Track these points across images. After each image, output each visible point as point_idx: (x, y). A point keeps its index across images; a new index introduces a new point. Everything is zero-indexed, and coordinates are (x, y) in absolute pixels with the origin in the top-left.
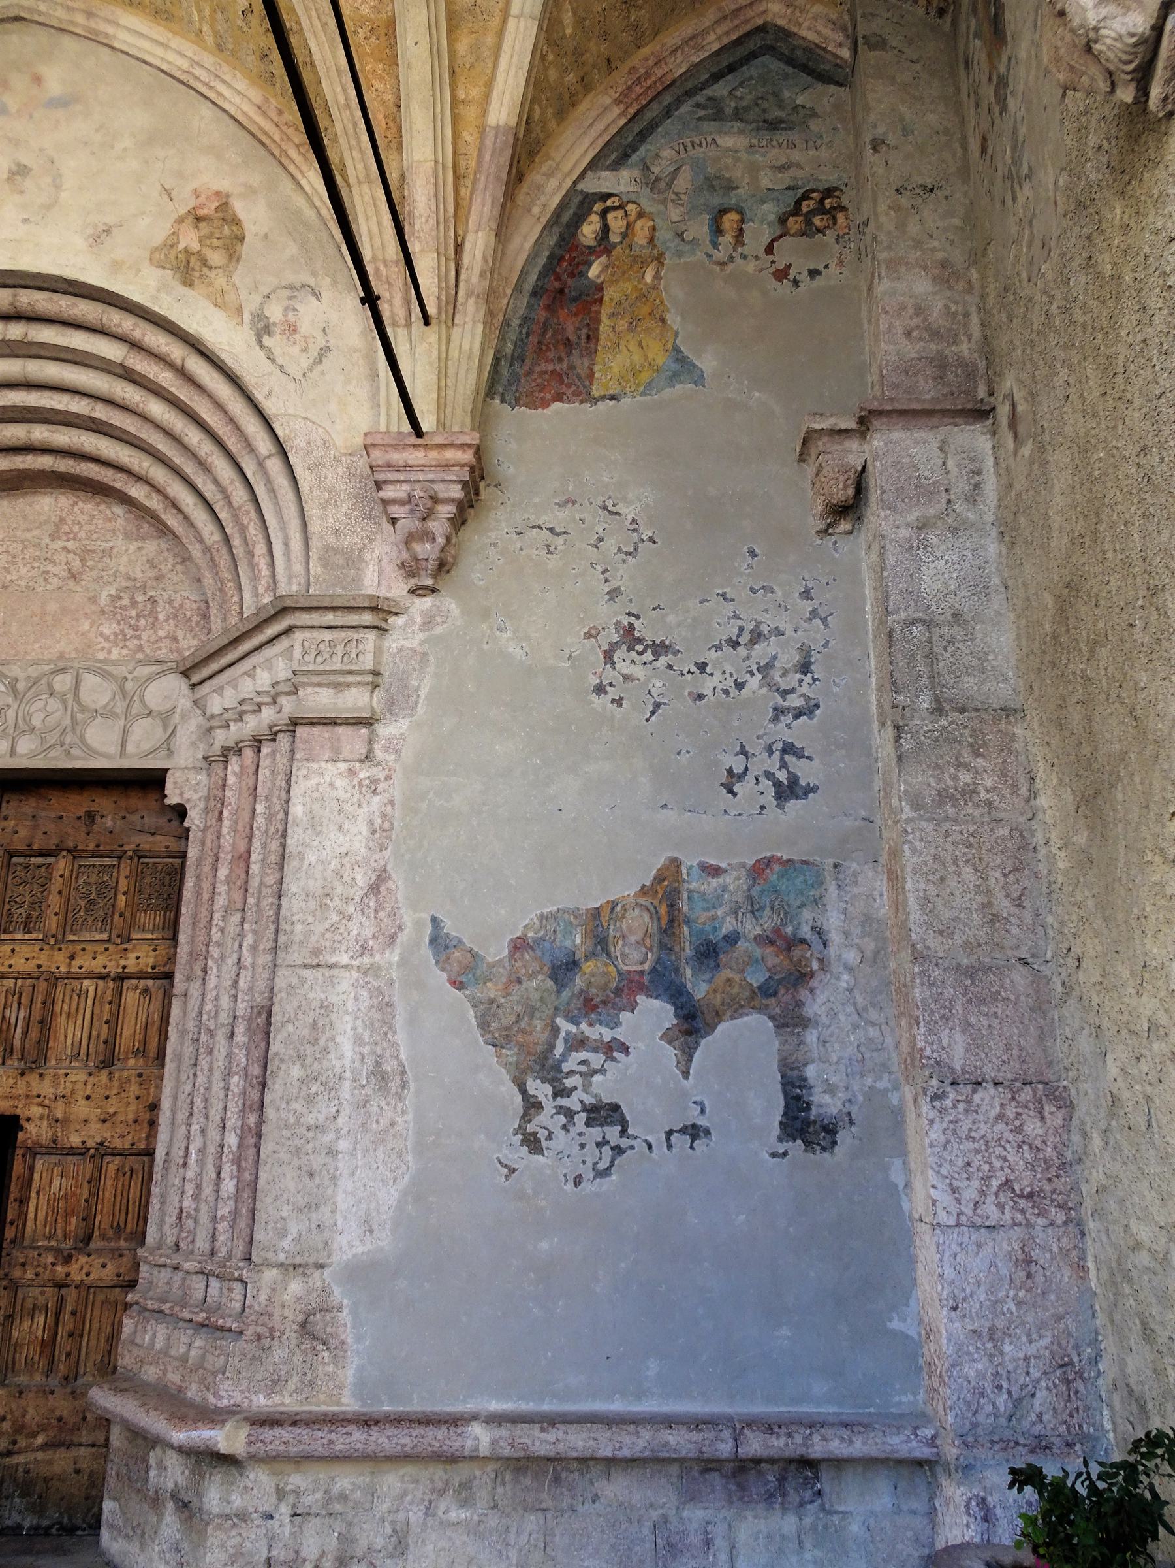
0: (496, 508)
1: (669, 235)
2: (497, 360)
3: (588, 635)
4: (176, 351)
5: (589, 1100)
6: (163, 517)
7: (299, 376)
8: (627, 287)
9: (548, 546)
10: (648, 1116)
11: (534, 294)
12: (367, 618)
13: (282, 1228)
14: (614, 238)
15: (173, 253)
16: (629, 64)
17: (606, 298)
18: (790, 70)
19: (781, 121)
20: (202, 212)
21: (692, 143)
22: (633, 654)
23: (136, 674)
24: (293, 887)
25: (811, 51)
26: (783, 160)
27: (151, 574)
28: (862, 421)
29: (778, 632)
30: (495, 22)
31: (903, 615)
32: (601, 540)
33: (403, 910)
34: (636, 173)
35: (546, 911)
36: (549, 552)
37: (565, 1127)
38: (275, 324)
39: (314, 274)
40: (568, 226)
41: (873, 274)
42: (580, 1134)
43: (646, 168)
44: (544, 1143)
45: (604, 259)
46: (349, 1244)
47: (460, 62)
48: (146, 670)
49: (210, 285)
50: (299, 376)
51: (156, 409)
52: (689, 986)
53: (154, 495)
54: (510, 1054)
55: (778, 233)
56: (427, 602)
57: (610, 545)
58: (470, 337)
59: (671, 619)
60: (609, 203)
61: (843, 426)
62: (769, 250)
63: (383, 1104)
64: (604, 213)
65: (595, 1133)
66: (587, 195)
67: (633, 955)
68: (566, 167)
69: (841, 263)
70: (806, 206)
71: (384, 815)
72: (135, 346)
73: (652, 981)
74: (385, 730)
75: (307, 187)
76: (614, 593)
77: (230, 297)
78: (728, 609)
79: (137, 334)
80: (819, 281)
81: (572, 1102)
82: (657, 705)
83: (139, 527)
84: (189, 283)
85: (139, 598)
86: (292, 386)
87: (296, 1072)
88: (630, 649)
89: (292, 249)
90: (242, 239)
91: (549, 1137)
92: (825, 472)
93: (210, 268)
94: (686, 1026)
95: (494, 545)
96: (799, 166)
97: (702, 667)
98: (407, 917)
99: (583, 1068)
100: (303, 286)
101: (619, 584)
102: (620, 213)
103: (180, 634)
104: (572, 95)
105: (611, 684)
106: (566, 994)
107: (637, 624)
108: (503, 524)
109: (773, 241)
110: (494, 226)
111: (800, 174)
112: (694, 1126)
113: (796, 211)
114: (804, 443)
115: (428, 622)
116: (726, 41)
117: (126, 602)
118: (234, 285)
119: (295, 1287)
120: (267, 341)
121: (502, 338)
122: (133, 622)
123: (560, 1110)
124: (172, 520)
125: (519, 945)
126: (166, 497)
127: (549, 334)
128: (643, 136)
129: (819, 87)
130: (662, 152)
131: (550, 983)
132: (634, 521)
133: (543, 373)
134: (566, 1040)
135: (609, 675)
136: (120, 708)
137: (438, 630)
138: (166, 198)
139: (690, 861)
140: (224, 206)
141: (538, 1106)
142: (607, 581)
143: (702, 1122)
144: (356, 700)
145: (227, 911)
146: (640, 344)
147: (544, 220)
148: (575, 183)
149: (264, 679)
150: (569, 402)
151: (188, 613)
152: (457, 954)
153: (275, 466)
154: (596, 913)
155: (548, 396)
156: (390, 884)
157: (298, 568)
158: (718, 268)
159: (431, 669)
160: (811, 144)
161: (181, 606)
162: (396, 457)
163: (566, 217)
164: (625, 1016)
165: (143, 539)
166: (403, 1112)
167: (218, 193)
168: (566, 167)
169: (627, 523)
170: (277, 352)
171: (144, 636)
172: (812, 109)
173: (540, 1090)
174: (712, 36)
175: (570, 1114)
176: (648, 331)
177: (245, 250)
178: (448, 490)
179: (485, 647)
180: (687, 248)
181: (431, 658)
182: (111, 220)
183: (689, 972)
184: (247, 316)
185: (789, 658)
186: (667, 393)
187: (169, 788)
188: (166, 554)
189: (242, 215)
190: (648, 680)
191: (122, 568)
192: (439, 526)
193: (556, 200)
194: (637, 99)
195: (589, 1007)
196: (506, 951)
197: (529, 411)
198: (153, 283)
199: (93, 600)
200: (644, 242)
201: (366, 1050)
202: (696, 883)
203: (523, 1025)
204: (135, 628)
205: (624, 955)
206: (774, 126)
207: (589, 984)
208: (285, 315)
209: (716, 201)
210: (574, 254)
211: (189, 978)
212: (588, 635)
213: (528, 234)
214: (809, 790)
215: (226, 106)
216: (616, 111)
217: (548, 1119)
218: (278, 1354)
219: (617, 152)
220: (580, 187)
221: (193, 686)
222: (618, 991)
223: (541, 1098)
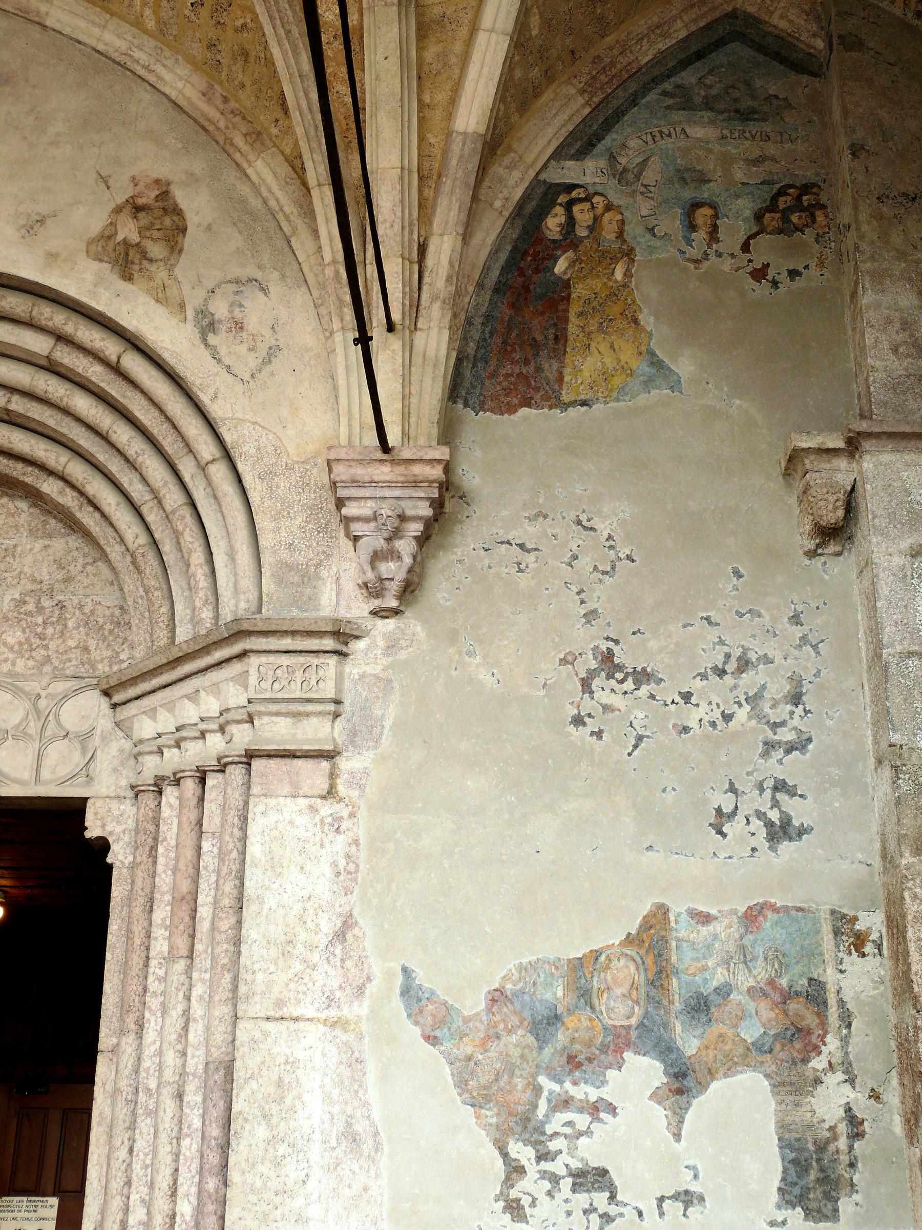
0: (461, 522)
1: (640, 230)
2: (459, 361)
3: (564, 661)
4: (111, 348)
5: (575, 1164)
6: (79, 515)
7: (247, 377)
8: (596, 284)
9: (519, 564)
10: (638, 1182)
11: (496, 290)
12: (329, 643)
14: (582, 232)
15: (111, 244)
16: (593, 53)
17: (573, 296)
18: (761, 58)
19: (753, 111)
20: (140, 201)
21: (661, 132)
22: (613, 682)
23: (50, 690)
24: (252, 931)
25: (782, 39)
26: (757, 153)
27: (60, 576)
28: (850, 441)
29: (767, 660)
30: (464, 32)
31: (899, 648)
32: (575, 557)
33: (372, 959)
34: (603, 163)
35: (525, 961)
36: (520, 571)
37: (550, 1194)
38: (220, 321)
39: (261, 267)
40: (531, 216)
41: (856, 283)
42: (566, 1201)
43: (612, 158)
44: (528, 1211)
45: (570, 254)
47: (426, 69)
48: (60, 687)
49: (150, 279)
50: (247, 377)
51: (82, 404)
52: (679, 1043)
53: (68, 490)
54: (490, 1115)
55: (755, 229)
56: (391, 624)
57: (585, 563)
58: (435, 340)
59: (653, 644)
60: (574, 194)
61: (831, 445)
62: (746, 248)
63: (355, 1167)
64: (569, 206)
65: (582, 1199)
66: (551, 185)
67: (619, 1009)
68: (529, 159)
69: (821, 264)
70: (782, 202)
71: (348, 856)
73: (639, 1037)
75: (254, 177)
76: (591, 616)
77: (172, 292)
78: (712, 634)
79: (69, 329)
80: (800, 283)
81: (557, 1167)
82: (640, 738)
83: (45, 523)
84: (127, 277)
85: (46, 603)
86: (239, 387)
87: (262, 1132)
88: (610, 676)
89: (238, 241)
90: (184, 230)
91: (533, 1204)
92: (812, 491)
93: (151, 260)
94: (676, 1085)
95: (460, 561)
96: (774, 160)
97: (687, 697)
98: (376, 967)
99: (568, 1130)
100: (250, 280)
101: (596, 606)
102: (587, 206)
103: (92, 644)
104: (535, 88)
105: (589, 715)
106: (548, 1051)
107: (616, 649)
108: (469, 539)
109: (749, 238)
110: (461, 231)
111: (775, 168)
112: (687, 1192)
113: (772, 207)
114: (790, 460)
115: (391, 647)
116: (694, 28)
117: (31, 607)
118: (176, 279)
120: (211, 338)
121: (465, 339)
122: (39, 630)
123: (544, 1175)
124: (88, 518)
125: (497, 998)
126: (82, 493)
127: (514, 334)
128: (608, 125)
129: (793, 77)
130: (629, 142)
131: (531, 1039)
132: (610, 537)
133: (507, 376)
134: (549, 1101)
135: (587, 705)
136: (33, 728)
137: (403, 655)
138: (103, 186)
139: (678, 908)
140: (165, 195)
141: (520, 1170)
142: (582, 602)
143: (695, 1187)
144: (315, 731)
145: (170, 958)
146: (612, 346)
147: (506, 214)
148: (538, 174)
149: (211, 705)
150: (538, 407)
151: (101, 621)
152: (430, 1007)
153: (219, 472)
154: (577, 965)
155: (515, 401)
156: (356, 931)
157: (247, 582)
158: (692, 266)
159: (396, 697)
160: (786, 136)
161: (92, 612)
162: (360, 472)
163: (529, 208)
164: (611, 1074)
165: (50, 536)
166: (377, 1176)
167: (157, 182)
168: (529, 159)
169: (603, 539)
170: (223, 351)
171: (53, 645)
172: (786, 99)
173: (522, 1153)
174: (679, 24)
175: (555, 1179)
176: (621, 333)
177: (188, 242)
178: (415, 507)
179: (454, 673)
180: (659, 243)
181: (397, 686)
182: (43, 209)
183: (679, 1028)
184: (190, 314)
185: (778, 688)
186: (643, 399)
187: (90, 819)
188: (75, 553)
189: (183, 204)
190: (629, 712)
191: (26, 569)
192: (406, 547)
193: (518, 193)
194: (602, 88)
196: (483, 1005)
197: (495, 417)
198: (89, 277)
200: (612, 236)
201: (336, 1109)
202: (682, 929)
203: (502, 1084)
204: (42, 637)
205: (610, 1010)
206: (745, 116)
207: (573, 1040)
208: (231, 312)
209: (688, 194)
210: (539, 248)
211: (122, 1032)
212: (564, 661)
213: (491, 229)
214: (803, 831)
215: (167, 90)
216: (580, 100)
217: (530, 1185)
219: (580, 143)
220: (542, 177)
221: (114, 706)
222: (604, 1049)
223: (524, 1162)
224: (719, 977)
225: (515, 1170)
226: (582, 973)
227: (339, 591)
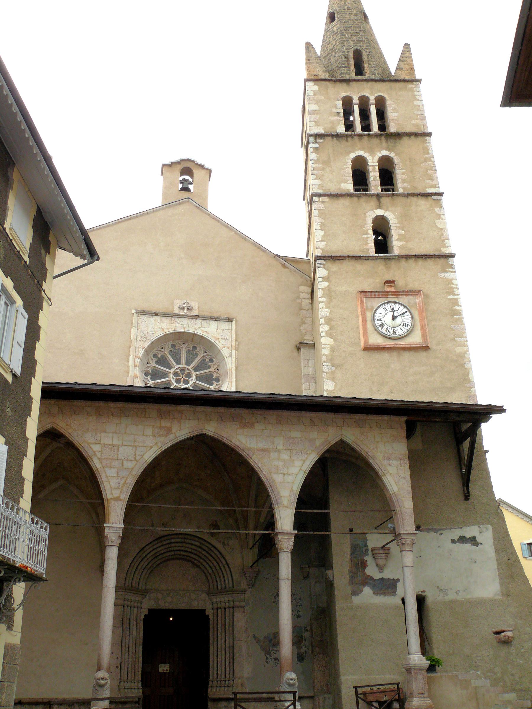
4: (210, 547)
13: (237, 673)
24: (235, 629)
51: (204, 552)
56: (250, 589)
58: (256, 549)
72: (201, 543)
74: (245, 608)
81: (272, 658)
84: (212, 537)
87: (238, 654)
115: (251, 593)
125: (265, 637)
144: (242, 604)
162: (248, 570)
173: (268, 656)
185: (299, 598)
192: (253, 580)
217: (269, 660)
225: (267, 658)
227: (244, 585)
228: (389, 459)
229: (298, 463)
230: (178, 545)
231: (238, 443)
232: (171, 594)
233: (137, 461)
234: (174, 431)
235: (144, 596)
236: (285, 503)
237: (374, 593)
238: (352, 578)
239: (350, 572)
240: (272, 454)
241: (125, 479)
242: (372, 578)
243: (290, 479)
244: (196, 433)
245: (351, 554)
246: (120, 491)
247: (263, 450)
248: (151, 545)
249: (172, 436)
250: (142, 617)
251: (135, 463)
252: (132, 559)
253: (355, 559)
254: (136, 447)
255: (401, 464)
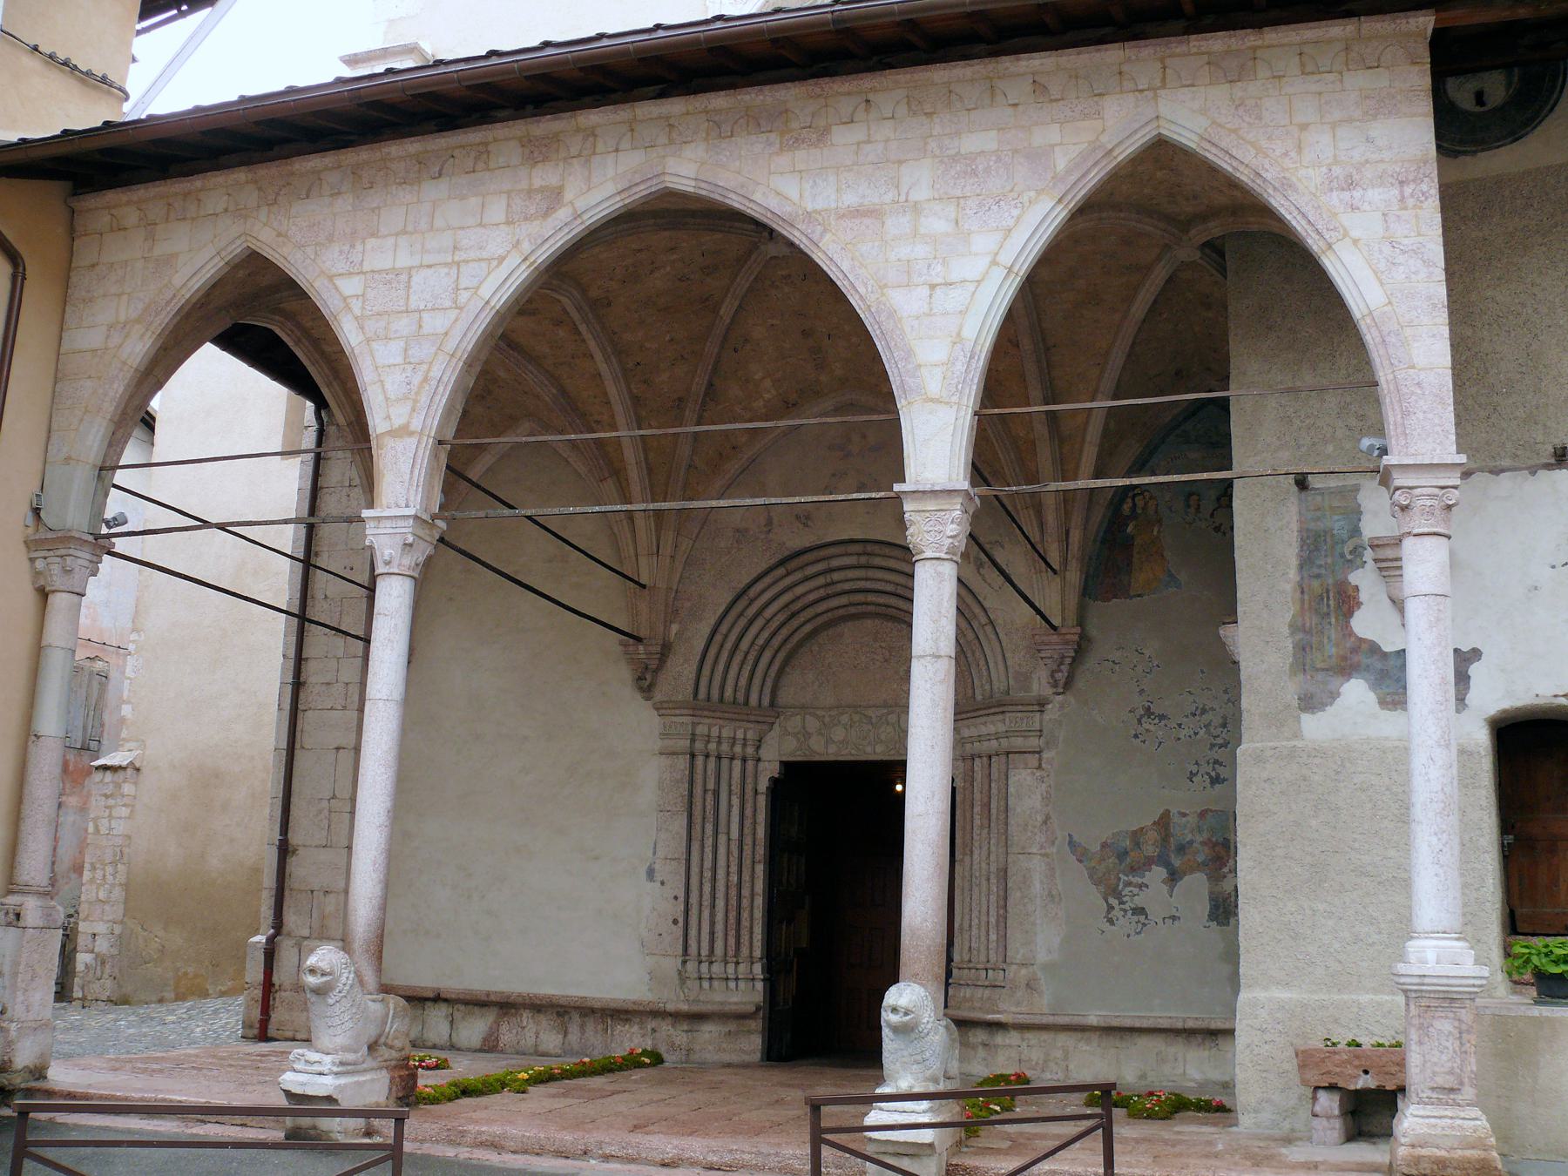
13: (1017, 951)
14: (1139, 511)
24: (1012, 821)
29: (1212, 709)
46: (1042, 957)
56: (1060, 697)
57: (1139, 669)
58: (1074, 576)
62: (1212, 515)
65: (1135, 918)
67: (1150, 850)
74: (1045, 755)
78: (1191, 699)
81: (1126, 907)
115: (1062, 707)
119: (1024, 971)
125: (1104, 845)
135: (1140, 730)
139: (1174, 811)
144: (1033, 742)
145: (982, 826)
149: (992, 729)
153: (989, 629)
154: (1134, 833)
157: (1003, 678)
175: (1125, 911)
185: (1217, 721)
192: (1064, 668)
195: (1133, 870)
199: (897, 672)
202: (1176, 819)
211: (964, 854)
214: (1224, 780)
217: (1116, 913)
218: (1019, 994)
224: (1189, 837)
225: (1111, 908)
226: (1137, 836)
227: (1040, 684)
228: (1350, 184)
229: (984, 243)
230: (850, 574)
231: (773, 203)
232: (845, 719)
233: (461, 309)
234: (569, 195)
235: (765, 727)
236: (933, 384)
237: (1383, 703)
238: (1302, 649)
239: (1294, 628)
240: (889, 222)
241: (425, 367)
242: (1374, 648)
243: (952, 300)
244: (642, 191)
245: (1301, 567)
246: (409, 404)
247: (857, 213)
248: (767, 580)
249: (563, 214)
250: (763, 785)
251: (453, 314)
252: (713, 621)
253: (1316, 583)
254: (458, 264)
255: (1402, 199)
